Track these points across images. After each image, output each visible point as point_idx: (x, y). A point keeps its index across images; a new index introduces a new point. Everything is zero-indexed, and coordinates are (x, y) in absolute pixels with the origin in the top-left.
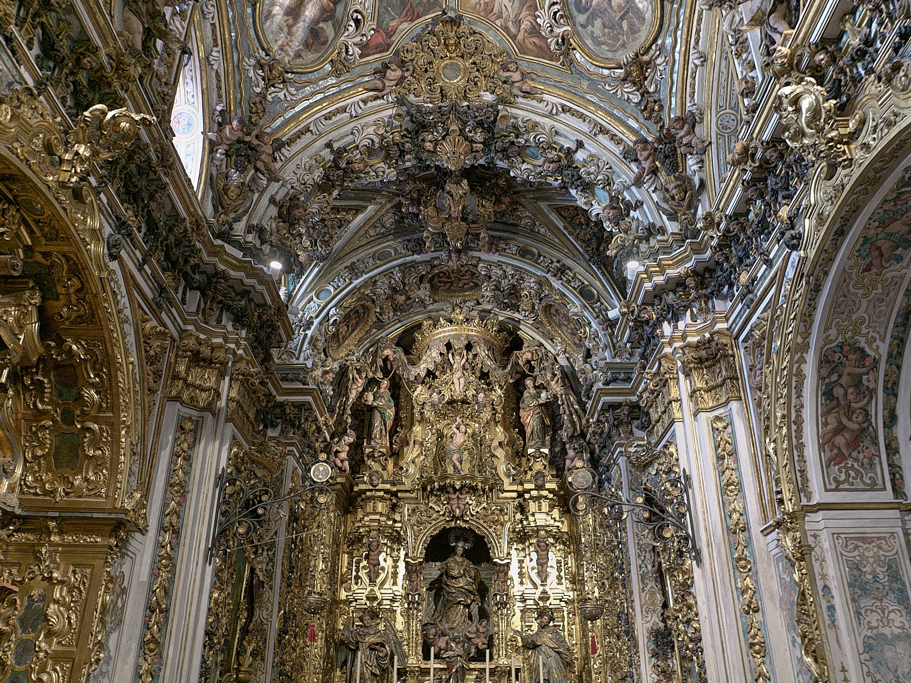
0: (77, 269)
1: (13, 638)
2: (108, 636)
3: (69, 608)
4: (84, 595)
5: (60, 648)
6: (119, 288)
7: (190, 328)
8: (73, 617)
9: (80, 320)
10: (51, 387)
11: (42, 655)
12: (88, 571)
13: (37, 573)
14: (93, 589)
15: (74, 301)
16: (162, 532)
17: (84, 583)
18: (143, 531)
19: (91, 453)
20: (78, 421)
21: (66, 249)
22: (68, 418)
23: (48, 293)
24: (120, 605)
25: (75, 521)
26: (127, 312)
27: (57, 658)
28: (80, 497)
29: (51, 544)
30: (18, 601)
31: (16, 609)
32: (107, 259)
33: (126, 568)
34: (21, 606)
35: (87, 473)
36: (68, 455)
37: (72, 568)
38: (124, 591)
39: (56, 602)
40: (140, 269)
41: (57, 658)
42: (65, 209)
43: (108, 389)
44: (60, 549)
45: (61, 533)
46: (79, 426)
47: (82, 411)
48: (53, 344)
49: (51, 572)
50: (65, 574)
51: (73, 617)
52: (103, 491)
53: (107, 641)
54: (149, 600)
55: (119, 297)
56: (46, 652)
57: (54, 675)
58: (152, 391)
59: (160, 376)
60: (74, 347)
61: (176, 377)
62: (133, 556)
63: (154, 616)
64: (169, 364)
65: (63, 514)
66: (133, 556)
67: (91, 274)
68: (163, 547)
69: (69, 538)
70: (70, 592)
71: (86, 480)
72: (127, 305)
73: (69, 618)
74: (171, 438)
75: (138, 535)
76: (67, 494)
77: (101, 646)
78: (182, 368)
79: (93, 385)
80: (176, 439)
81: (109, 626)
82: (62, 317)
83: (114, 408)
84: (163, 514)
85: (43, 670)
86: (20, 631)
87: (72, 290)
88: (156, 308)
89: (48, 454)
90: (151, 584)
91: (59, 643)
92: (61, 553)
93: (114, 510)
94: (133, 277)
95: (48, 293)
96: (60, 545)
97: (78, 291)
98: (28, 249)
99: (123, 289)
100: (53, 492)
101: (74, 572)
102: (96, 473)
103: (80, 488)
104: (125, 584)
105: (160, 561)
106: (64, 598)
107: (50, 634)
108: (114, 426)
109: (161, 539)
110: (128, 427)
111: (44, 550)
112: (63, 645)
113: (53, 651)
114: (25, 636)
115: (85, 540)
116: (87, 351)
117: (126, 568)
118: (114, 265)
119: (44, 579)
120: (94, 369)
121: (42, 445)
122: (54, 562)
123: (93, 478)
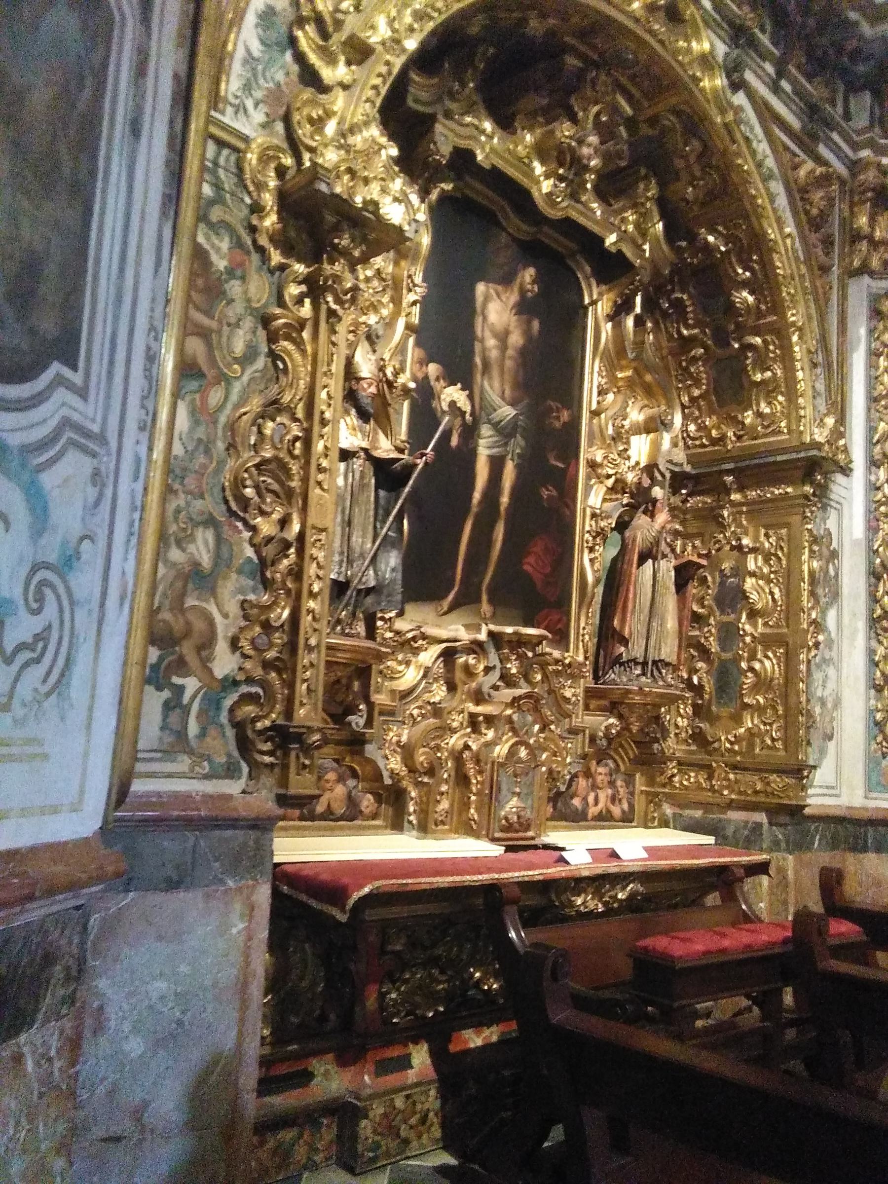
0: (694, 123)
1: (712, 621)
2: (824, 612)
3: (769, 581)
4: (784, 562)
5: (768, 631)
6: (752, 129)
7: (865, 153)
8: (776, 591)
9: (711, 197)
10: (693, 304)
11: (748, 639)
12: (784, 531)
13: (724, 542)
14: (794, 554)
15: (698, 174)
16: (874, 469)
17: (782, 548)
18: (846, 471)
19: (758, 377)
20: (734, 339)
21: (673, 100)
22: (722, 339)
23: (665, 176)
24: (832, 572)
25: (758, 470)
26: (770, 162)
27: (767, 642)
28: (755, 438)
29: (733, 504)
30: (709, 578)
31: (708, 587)
32: (729, 93)
33: (831, 524)
34: (714, 582)
35: (758, 405)
36: (730, 387)
37: (763, 531)
38: (834, 555)
39: (753, 574)
40: (776, 89)
41: (767, 642)
42: (661, 42)
43: (765, 284)
44: (744, 509)
45: (741, 489)
46: (736, 346)
47: (738, 325)
48: (684, 244)
49: (739, 539)
50: (756, 539)
51: (776, 591)
52: (783, 424)
53: (824, 618)
54: (871, 563)
55: (755, 144)
56: (752, 635)
57: (767, 664)
58: (825, 269)
59: (832, 243)
60: (711, 239)
61: (855, 237)
62: (838, 506)
63: (881, 584)
64: (843, 221)
65: (739, 465)
66: (838, 506)
67: (713, 123)
68: (878, 489)
69: (752, 494)
70: (767, 560)
71: (759, 414)
72: (768, 151)
73: (772, 593)
74: (863, 331)
75: (839, 478)
76: (739, 438)
77: (818, 625)
78: (863, 220)
79: (744, 284)
80: (871, 332)
81: (823, 600)
82: (687, 202)
83: (777, 308)
84: (870, 444)
85: (752, 657)
86: (718, 613)
87: (692, 159)
88: (808, 140)
89: (707, 391)
90: (870, 541)
91: (766, 624)
92: (748, 512)
93: (804, 447)
94: (766, 104)
95: (665, 176)
96: (741, 504)
97: (701, 156)
98: (631, 123)
99: (758, 130)
100: (722, 439)
101: (767, 536)
102: (769, 403)
103: (753, 427)
104: (835, 544)
105: (876, 509)
106: (761, 569)
107: (753, 614)
108: (781, 332)
109: (873, 478)
110: (800, 329)
111: (726, 513)
112: (771, 627)
113: (762, 634)
114: (725, 619)
115: (772, 493)
116: (727, 240)
117: (831, 524)
118: (740, 99)
119: (733, 548)
120: (741, 262)
121: (697, 383)
122: (740, 525)
123: (767, 410)
